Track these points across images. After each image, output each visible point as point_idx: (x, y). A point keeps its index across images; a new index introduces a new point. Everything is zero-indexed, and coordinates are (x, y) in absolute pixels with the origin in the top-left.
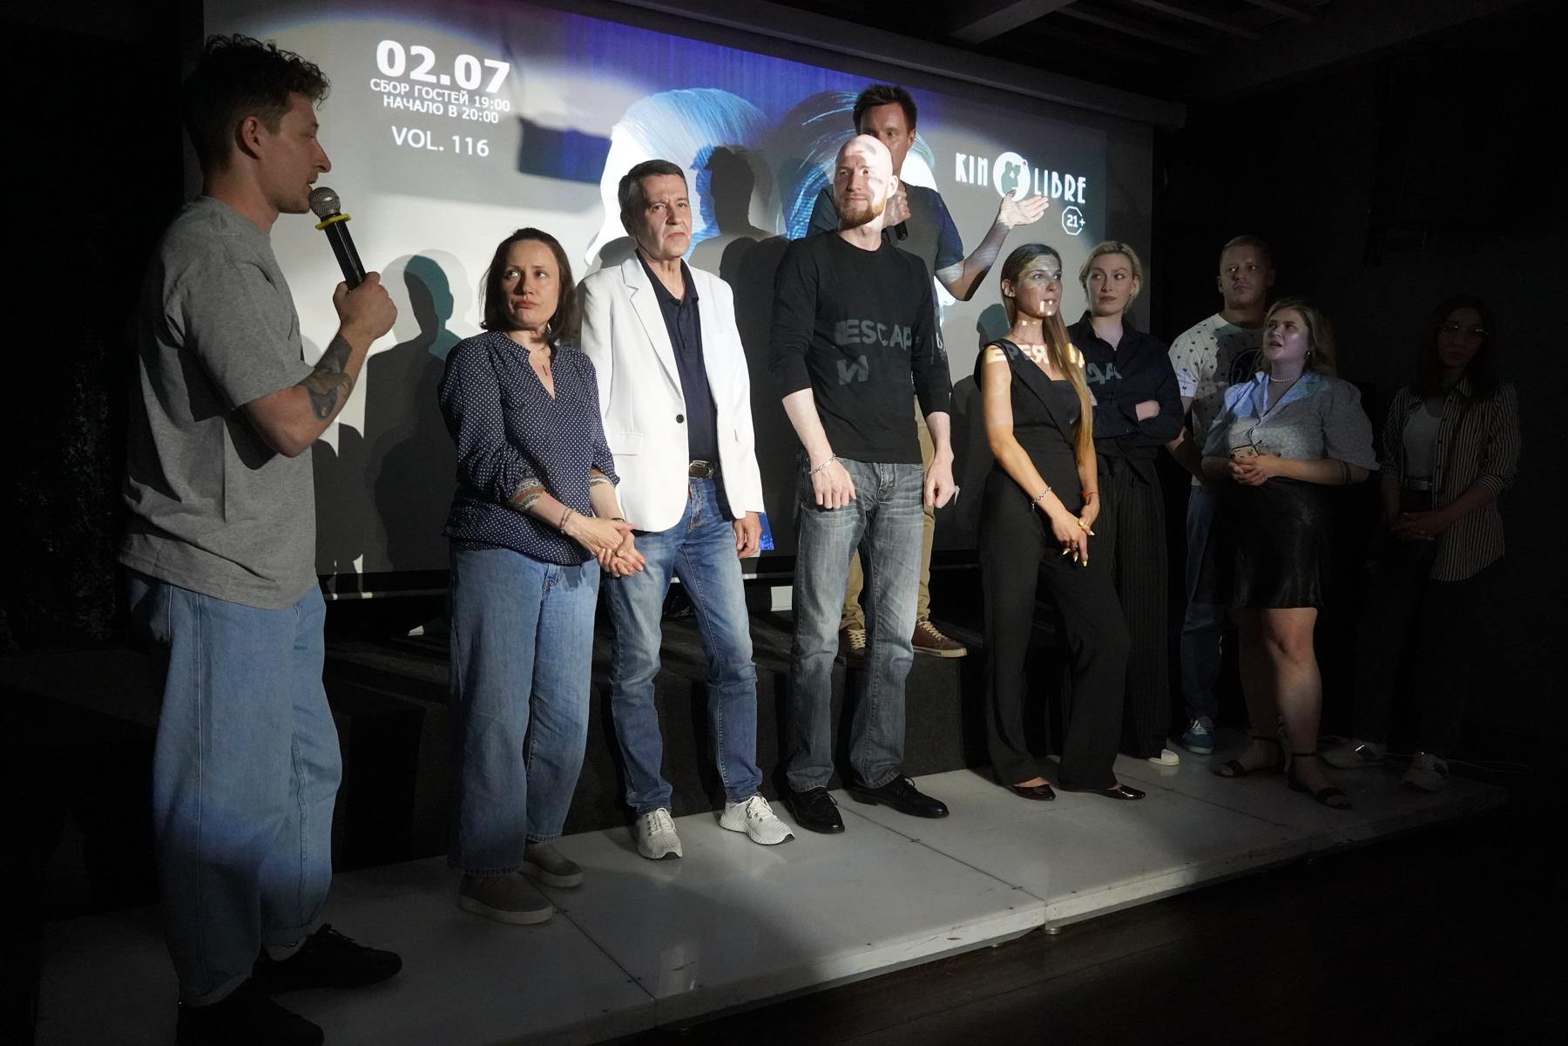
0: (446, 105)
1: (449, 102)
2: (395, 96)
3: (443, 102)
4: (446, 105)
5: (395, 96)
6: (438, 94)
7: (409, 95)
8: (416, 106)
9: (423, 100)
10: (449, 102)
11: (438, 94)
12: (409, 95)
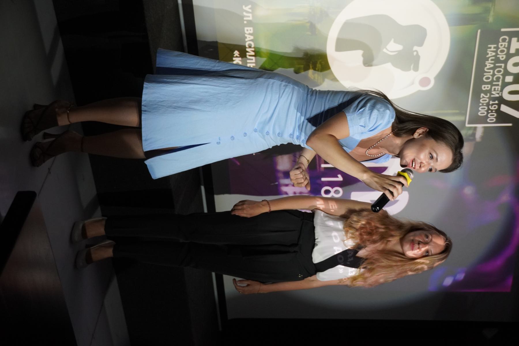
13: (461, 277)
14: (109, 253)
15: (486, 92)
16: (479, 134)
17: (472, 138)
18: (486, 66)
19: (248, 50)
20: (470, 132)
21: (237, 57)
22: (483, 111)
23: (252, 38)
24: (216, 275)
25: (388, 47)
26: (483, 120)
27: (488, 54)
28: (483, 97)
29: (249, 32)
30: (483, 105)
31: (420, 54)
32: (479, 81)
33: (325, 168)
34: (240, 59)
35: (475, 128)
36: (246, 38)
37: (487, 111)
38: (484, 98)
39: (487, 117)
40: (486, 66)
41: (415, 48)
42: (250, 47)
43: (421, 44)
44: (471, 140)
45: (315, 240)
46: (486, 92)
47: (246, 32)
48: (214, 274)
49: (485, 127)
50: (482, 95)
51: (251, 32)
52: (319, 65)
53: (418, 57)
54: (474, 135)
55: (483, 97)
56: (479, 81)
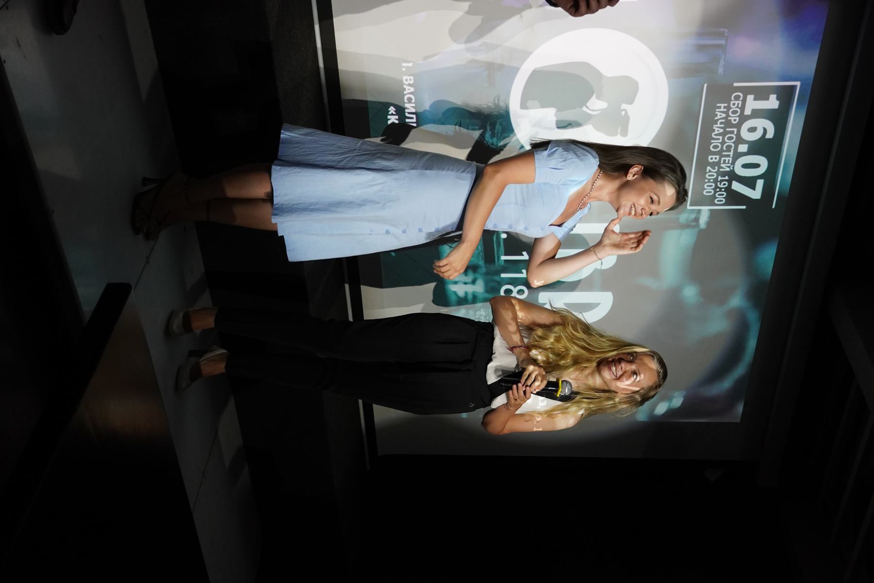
0: (719, 153)
1: (721, 156)
2: (727, 113)
3: (722, 150)
4: (719, 153)
5: (727, 113)
6: (729, 147)
7: (727, 123)
8: (717, 129)
9: (723, 134)
10: (721, 156)
11: (729, 147)
12: (727, 123)
13: (677, 402)
14: (221, 368)
15: (713, 165)
16: (704, 219)
17: (694, 224)
18: (714, 131)
19: (407, 105)
20: (693, 216)
21: (392, 114)
22: (709, 189)
23: (412, 89)
24: (363, 403)
25: (588, 104)
26: (711, 201)
27: (716, 115)
28: (710, 171)
29: (409, 82)
30: (709, 182)
31: (629, 114)
32: (705, 150)
33: (505, 261)
34: (397, 117)
35: (699, 211)
36: (405, 89)
37: (714, 189)
38: (711, 173)
39: (714, 197)
40: (714, 131)
41: (624, 106)
42: (410, 100)
43: (631, 101)
44: (694, 227)
45: (492, 354)
46: (713, 165)
47: (405, 82)
48: (360, 401)
49: (711, 210)
50: (709, 168)
51: (412, 82)
52: (498, 127)
53: (627, 118)
54: (697, 220)
55: (710, 171)
56: (705, 150)
